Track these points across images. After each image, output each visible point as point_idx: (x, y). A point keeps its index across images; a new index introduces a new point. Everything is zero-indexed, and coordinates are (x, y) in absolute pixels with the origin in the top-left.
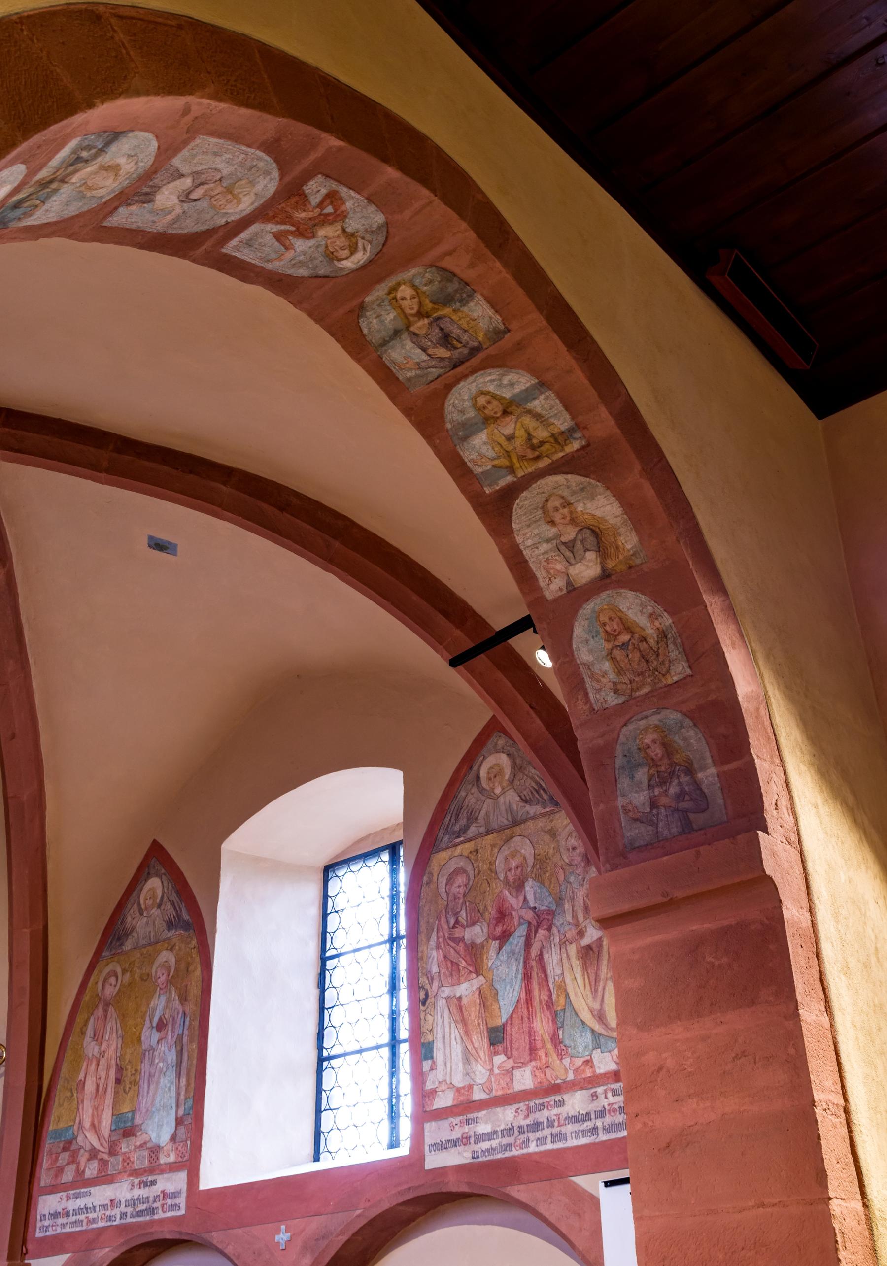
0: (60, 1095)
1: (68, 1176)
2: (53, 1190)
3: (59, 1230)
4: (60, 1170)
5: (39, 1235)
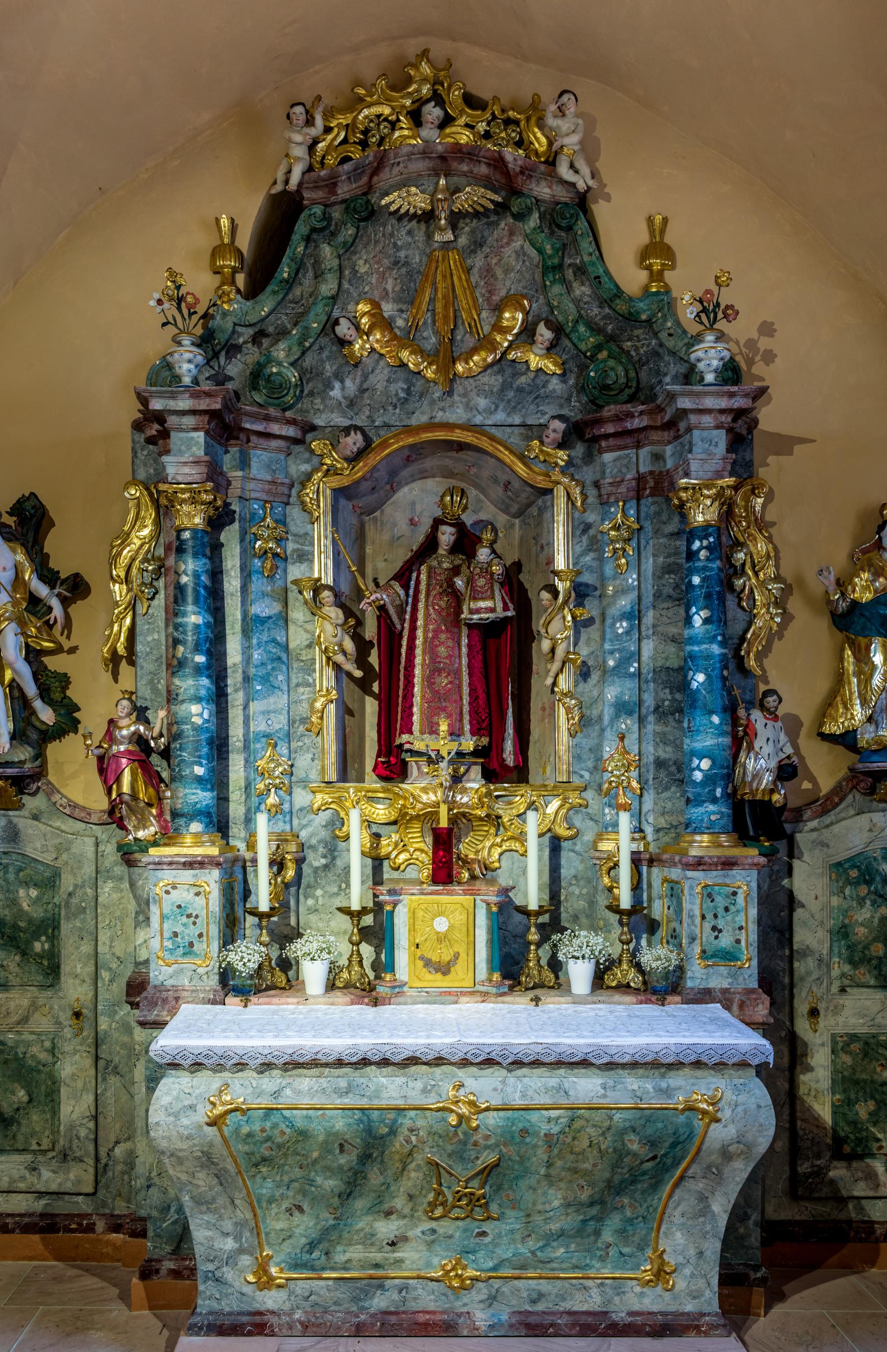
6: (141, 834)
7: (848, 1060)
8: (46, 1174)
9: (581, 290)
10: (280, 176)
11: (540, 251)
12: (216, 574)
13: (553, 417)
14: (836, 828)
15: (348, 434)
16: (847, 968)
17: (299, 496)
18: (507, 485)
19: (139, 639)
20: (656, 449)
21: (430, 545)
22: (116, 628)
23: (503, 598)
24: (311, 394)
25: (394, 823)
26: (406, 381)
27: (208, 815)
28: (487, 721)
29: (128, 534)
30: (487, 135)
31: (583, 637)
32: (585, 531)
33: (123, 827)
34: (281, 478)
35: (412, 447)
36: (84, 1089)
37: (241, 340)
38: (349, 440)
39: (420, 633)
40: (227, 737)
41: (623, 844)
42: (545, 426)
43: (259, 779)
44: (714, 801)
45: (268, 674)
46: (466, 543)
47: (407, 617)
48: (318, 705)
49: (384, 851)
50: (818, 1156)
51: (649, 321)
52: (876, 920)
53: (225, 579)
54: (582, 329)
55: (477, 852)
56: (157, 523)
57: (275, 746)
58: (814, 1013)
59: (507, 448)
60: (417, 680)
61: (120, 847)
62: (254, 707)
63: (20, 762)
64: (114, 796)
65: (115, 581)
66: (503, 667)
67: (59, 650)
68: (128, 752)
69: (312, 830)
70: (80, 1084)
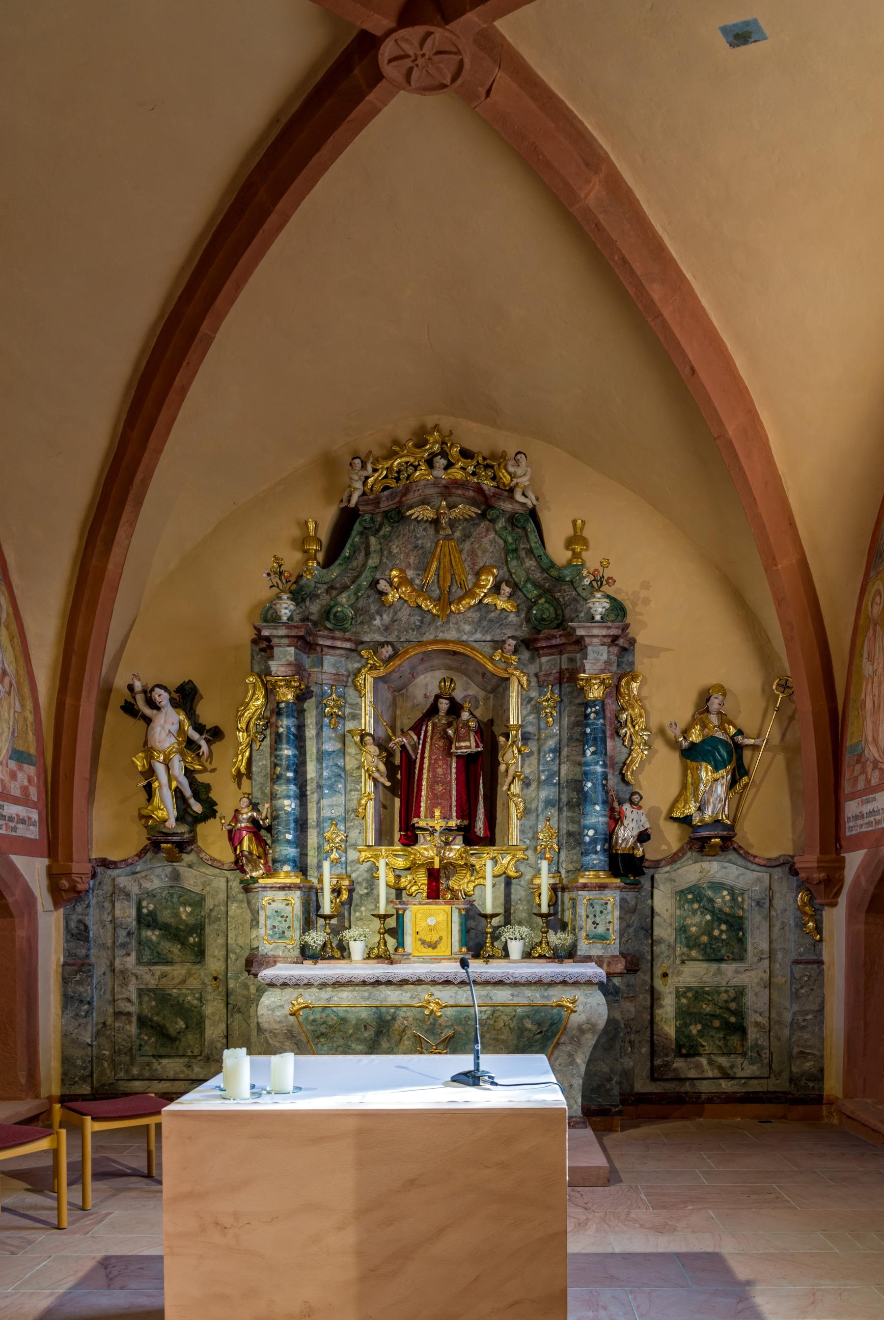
0: (852, 715)
1: (861, 785)
2: (853, 796)
3: (859, 830)
4: (856, 780)
5: (848, 834)
6: (254, 874)
7: (684, 1001)
8: (197, 1069)
9: (530, 563)
10: (345, 498)
11: (505, 542)
12: (301, 727)
13: (509, 637)
14: (680, 871)
15: (383, 647)
16: (685, 950)
17: (353, 682)
18: (484, 675)
19: (254, 764)
20: (571, 655)
21: (434, 710)
22: (240, 757)
23: (476, 741)
24: (362, 623)
25: (409, 869)
26: (420, 615)
28: (467, 811)
29: (248, 704)
30: (474, 474)
31: (527, 762)
32: (529, 702)
33: (243, 871)
34: (343, 671)
35: (424, 653)
36: (220, 1020)
37: (319, 592)
38: (384, 650)
39: (426, 760)
40: (307, 819)
41: (545, 881)
42: (504, 642)
43: (326, 844)
44: (596, 853)
45: (333, 784)
46: (455, 709)
47: (419, 751)
48: (363, 802)
49: (402, 885)
50: (667, 1055)
51: (572, 582)
52: (703, 923)
53: (307, 730)
54: (529, 586)
55: (460, 885)
56: (266, 697)
57: (336, 825)
58: (665, 975)
59: (481, 654)
60: (424, 788)
61: (241, 882)
62: (325, 802)
63: (182, 833)
64: (238, 852)
65: (239, 731)
66: (479, 781)
67: (205, 770)
68: (246, 827)
69: (359, 873)
70: (217, 1018)
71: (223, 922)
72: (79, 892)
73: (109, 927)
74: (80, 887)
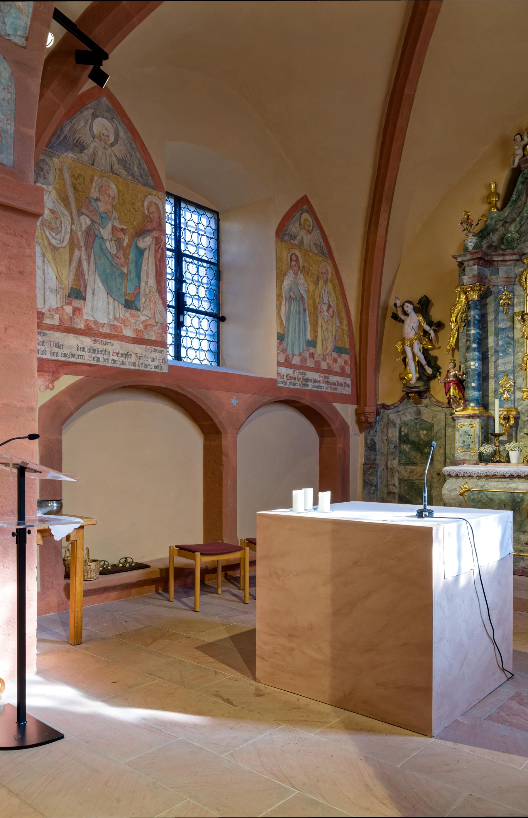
19: (460, 341)
27: (478, 400)
40: (488, 373)
43: (500, 388)
45: (505, 349)
53: (488, 316)
57: (508, 375)
62: (500, 361)
67: (434, 348)
71: (443, 439)
72: (370, 423)
73: (386, 442)
74: (370, 420)
